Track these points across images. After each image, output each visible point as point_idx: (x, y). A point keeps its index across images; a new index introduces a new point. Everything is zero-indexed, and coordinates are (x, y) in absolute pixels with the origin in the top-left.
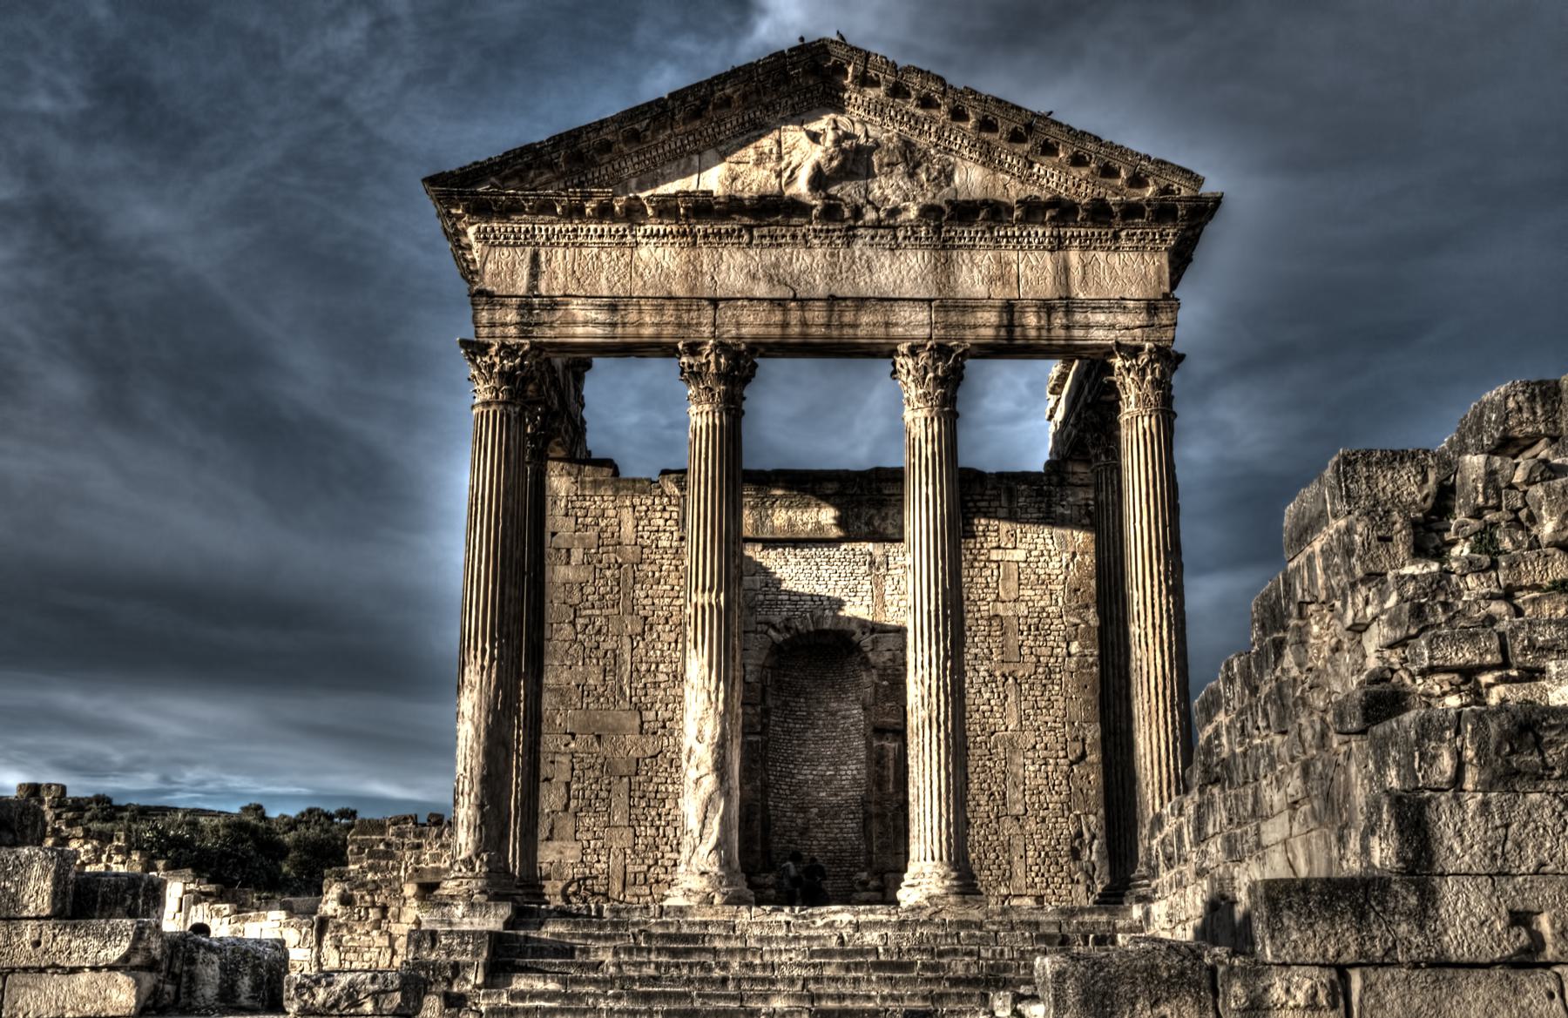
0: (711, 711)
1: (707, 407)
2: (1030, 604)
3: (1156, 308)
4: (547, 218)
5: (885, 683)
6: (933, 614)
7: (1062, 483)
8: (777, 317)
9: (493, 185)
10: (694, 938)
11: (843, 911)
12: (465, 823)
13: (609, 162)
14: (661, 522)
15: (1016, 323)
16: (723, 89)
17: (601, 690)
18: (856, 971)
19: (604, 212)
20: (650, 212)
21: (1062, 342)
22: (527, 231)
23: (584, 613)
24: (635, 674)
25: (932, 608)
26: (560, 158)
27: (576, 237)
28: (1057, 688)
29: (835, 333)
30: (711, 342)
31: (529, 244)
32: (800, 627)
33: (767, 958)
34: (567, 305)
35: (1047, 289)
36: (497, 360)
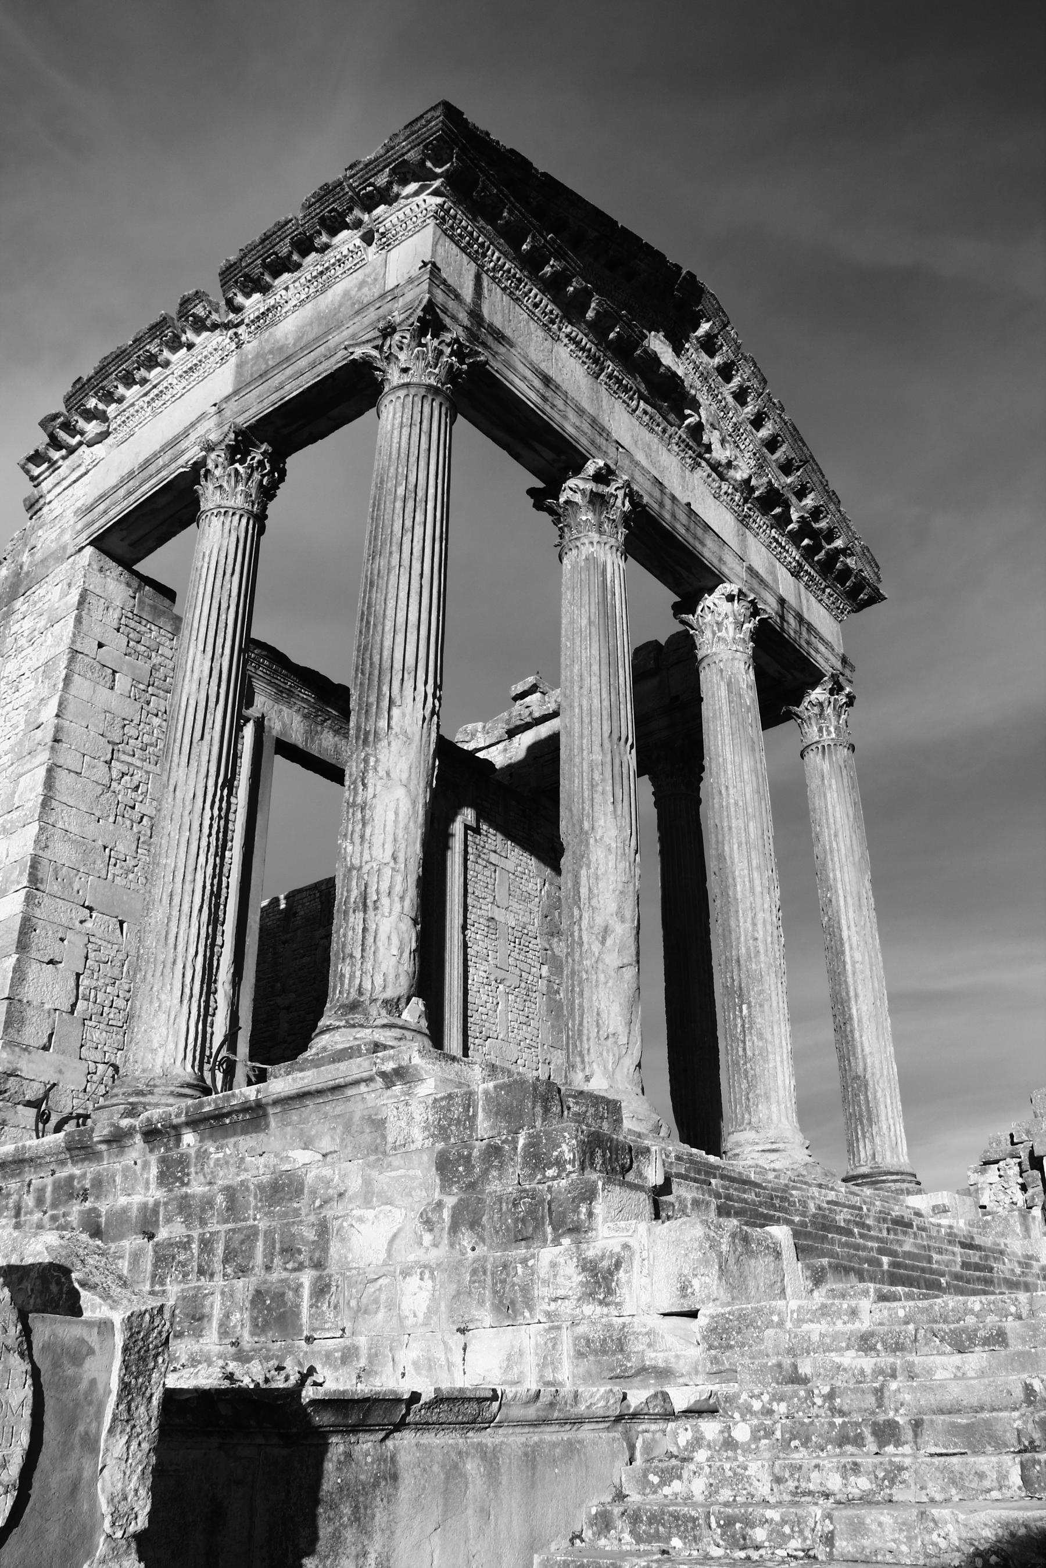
4: (506, 248)
12: (395, 941)
17: (131, 862)
19: (553, 287)
20: (590, 314)
22: (482, 245)
23: (124, 757)
27: (517, 288)
34: (512, 346)
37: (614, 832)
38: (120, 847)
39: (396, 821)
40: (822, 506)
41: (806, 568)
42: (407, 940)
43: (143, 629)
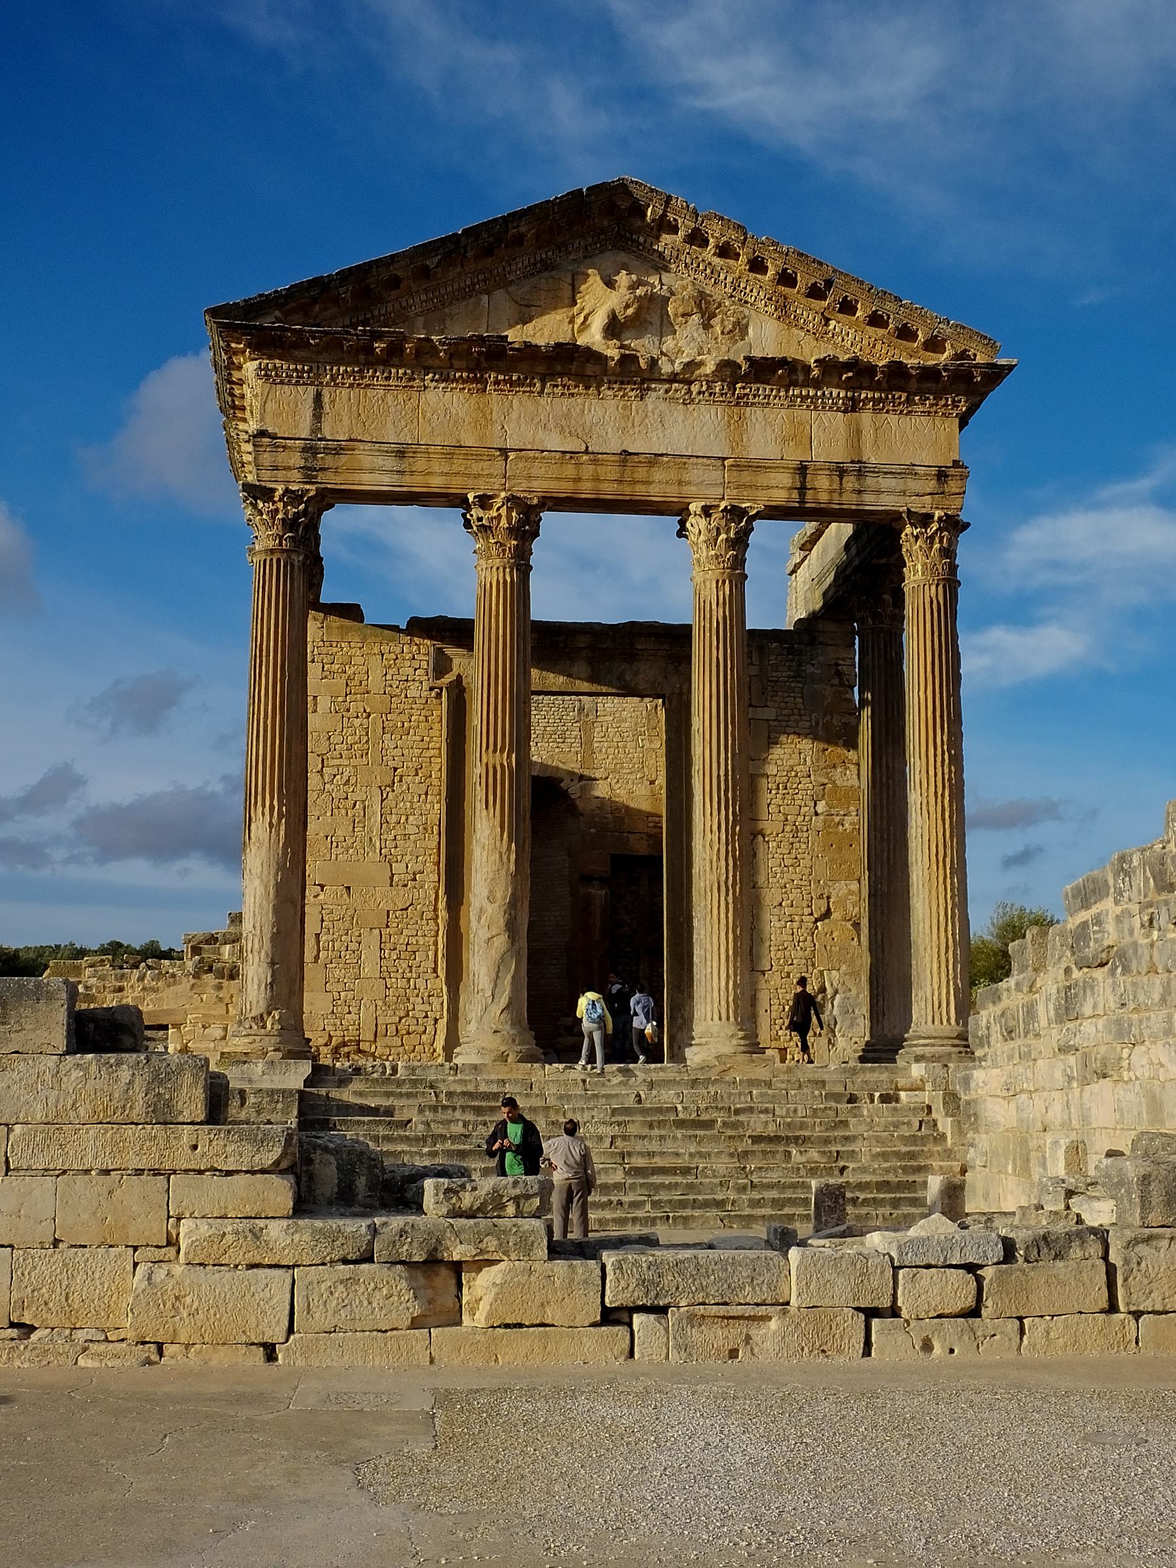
0: (504, 872)
1: (498, 562)
3: (948, 476)
5: (592, 830)
6: (722, 778)
8: (570, 470)
9: (278, 320)
12: (256, 980)
13: (397, 299)
14: (411, 670)
15: (809, 485)
16: (518, 227)
17: (350, 841)
18: (659, 1128)
21: (854, 507)
23: (332, 762)
24: (384, 826)
25: (722, 773)
26: (345, 292)
27: (363, 378)
28: (804, 846)
29: (627, 489)
30: (503, 494)
31: (312, 384)
34: (354, 450)
35: (840, 454)
36: (280, 505)
37: (487, 832)
38: (339, 832)
39: (255, 903)
40: (877, 311)
41: (863, 396)
42: (263, 977)
43: (335, 650)
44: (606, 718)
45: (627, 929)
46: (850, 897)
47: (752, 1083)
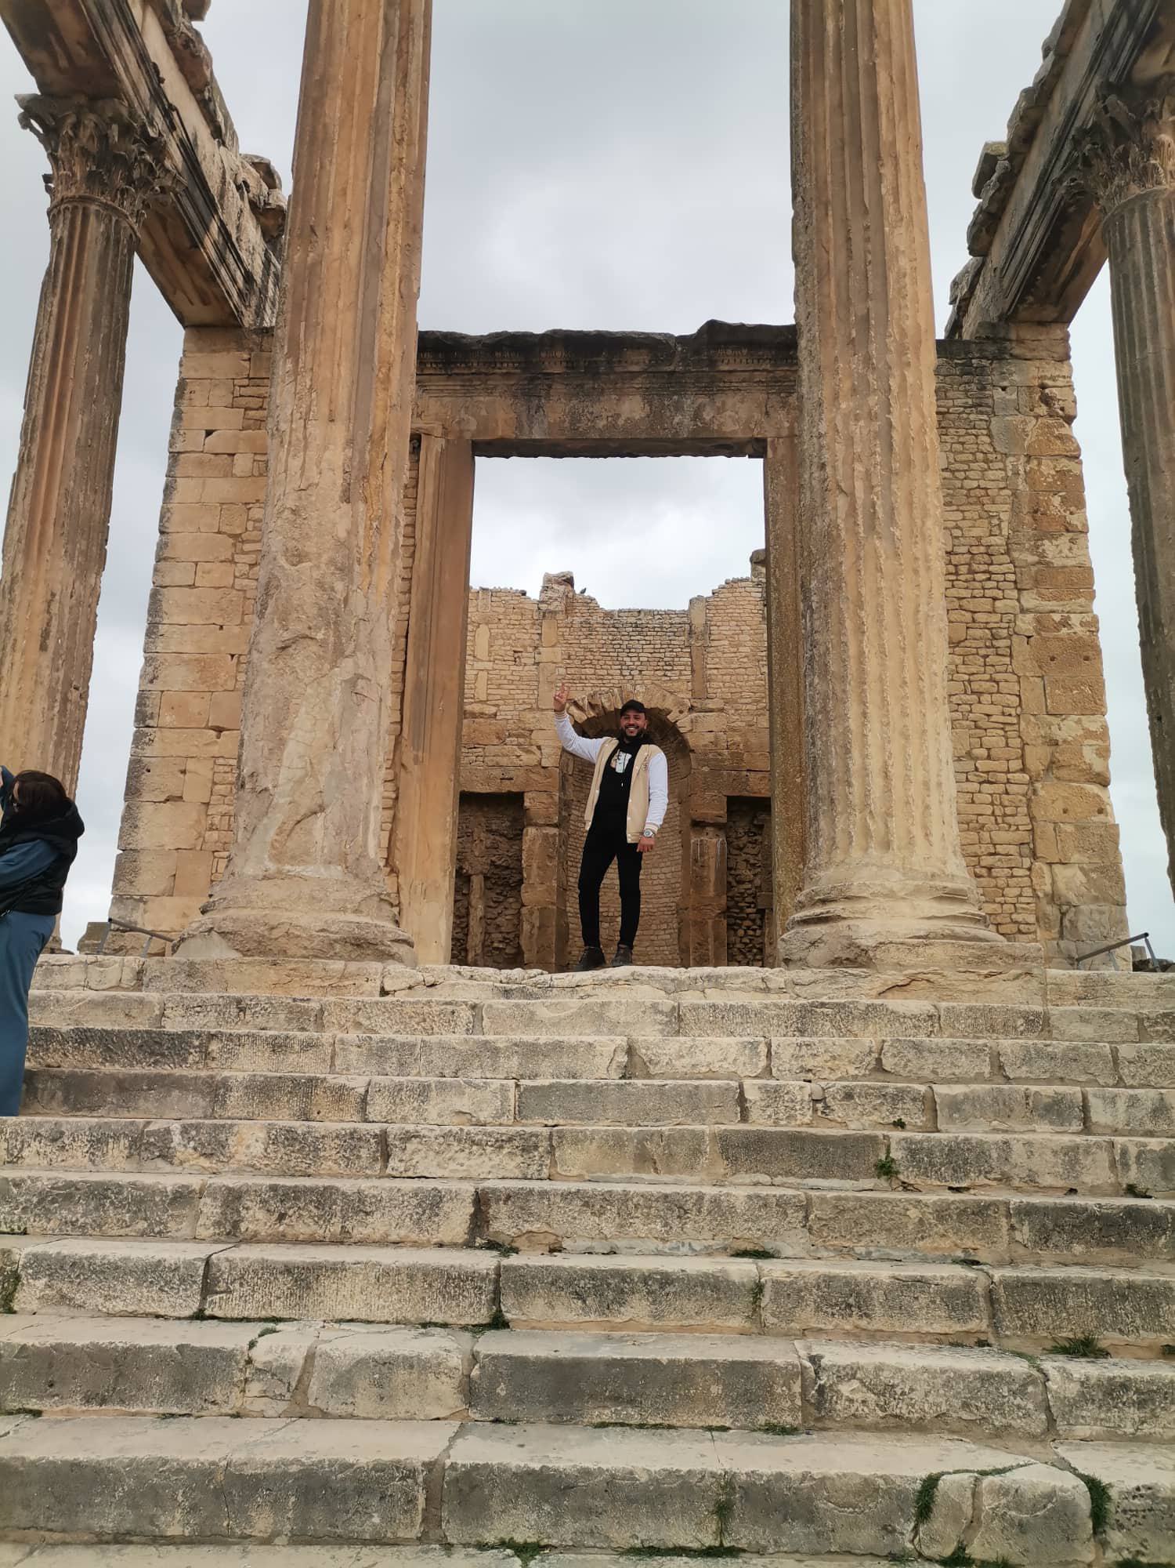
2: (957, 533)
5: (706, 769)
7: (999, 357)
10: (172, 1046)
11: (635, 978)
32: (607, 705)
33: (378, 1107)
44: (723, 642)
45: (750, 886)
46: (1086, 742)
47: (990, 1022)
